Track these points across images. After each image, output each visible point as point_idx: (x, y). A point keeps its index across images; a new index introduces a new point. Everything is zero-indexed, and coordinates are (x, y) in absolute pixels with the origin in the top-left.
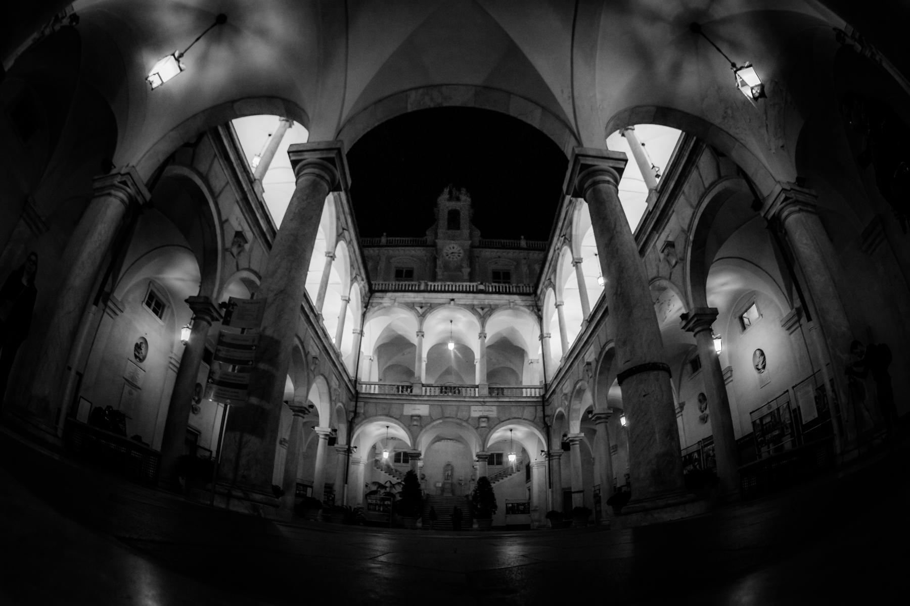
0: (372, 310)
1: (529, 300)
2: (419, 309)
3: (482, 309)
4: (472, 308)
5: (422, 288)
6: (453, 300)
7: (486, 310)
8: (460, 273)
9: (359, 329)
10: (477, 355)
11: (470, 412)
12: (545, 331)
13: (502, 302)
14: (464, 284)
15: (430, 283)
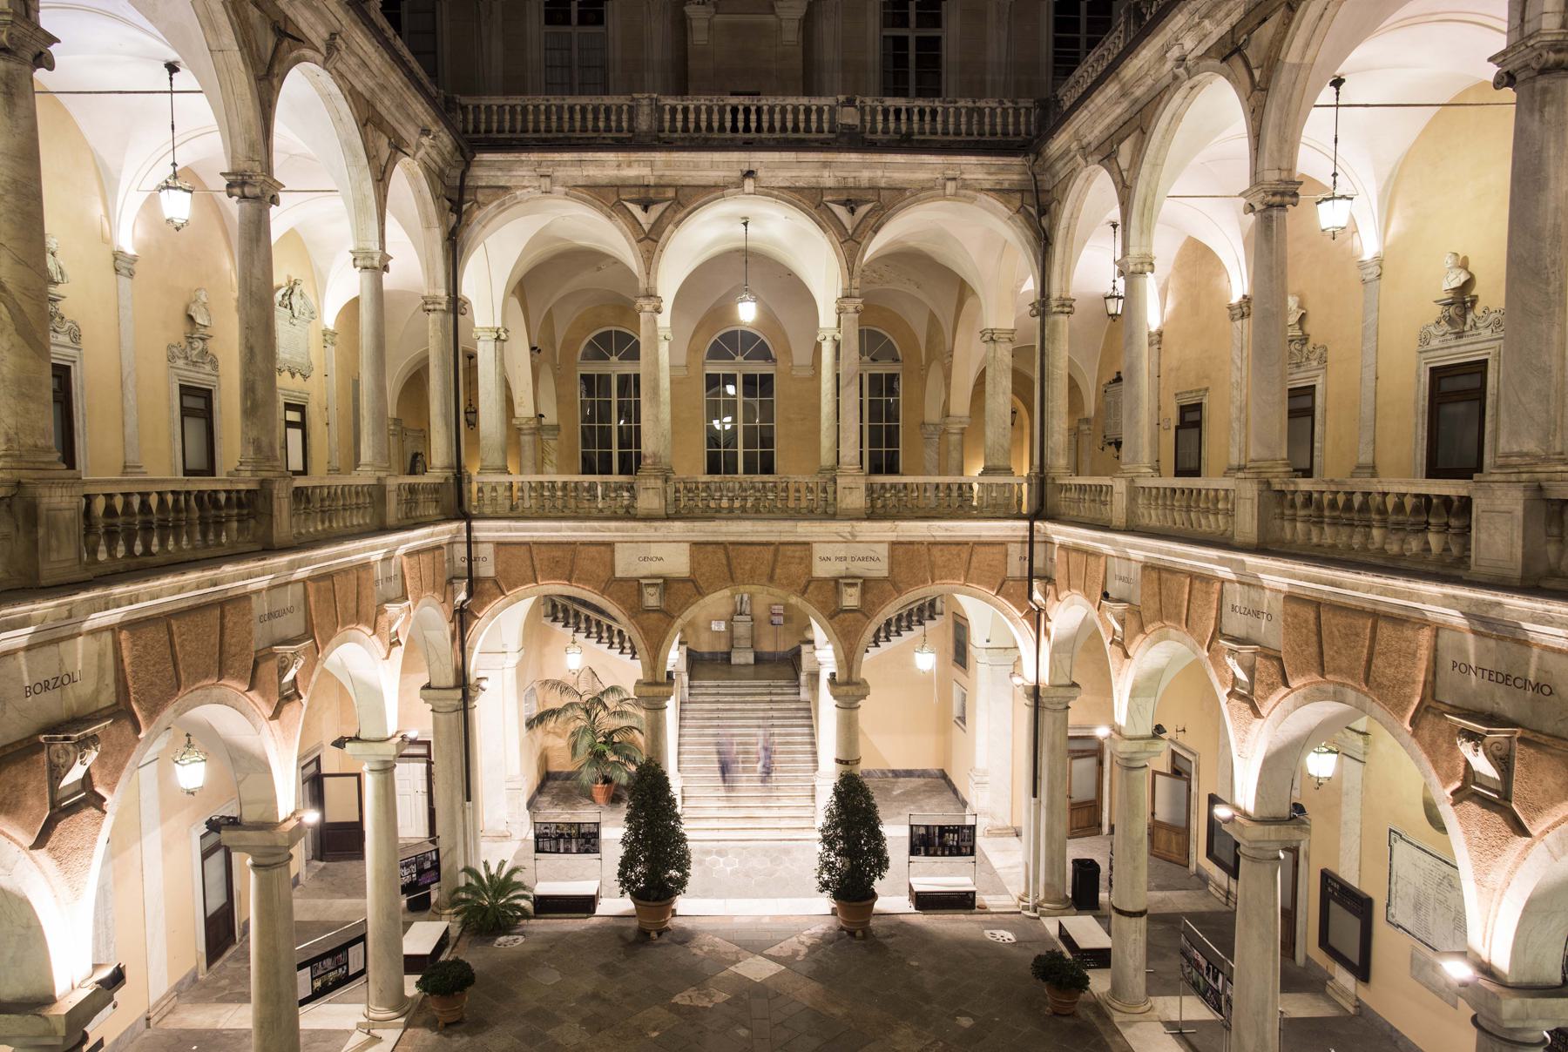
0: (478, 215)
1: (1011, 169)
2: (636, 210)
3: (851, 205)
4: (812, 200)
5: (643, 123)
6: (749, 174)
7: (863, 210)
8: (771, 18)
9: (442, 293)
10: (827, 318)
11: (809, 567)
12: (1055, 293)
13: (922, 175)
14: (791, 101)
15: (669, 101)
